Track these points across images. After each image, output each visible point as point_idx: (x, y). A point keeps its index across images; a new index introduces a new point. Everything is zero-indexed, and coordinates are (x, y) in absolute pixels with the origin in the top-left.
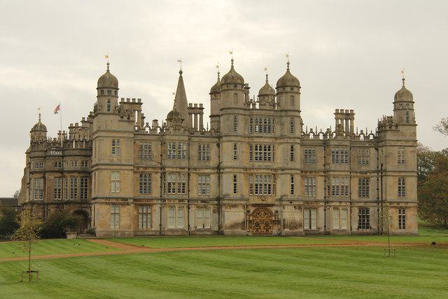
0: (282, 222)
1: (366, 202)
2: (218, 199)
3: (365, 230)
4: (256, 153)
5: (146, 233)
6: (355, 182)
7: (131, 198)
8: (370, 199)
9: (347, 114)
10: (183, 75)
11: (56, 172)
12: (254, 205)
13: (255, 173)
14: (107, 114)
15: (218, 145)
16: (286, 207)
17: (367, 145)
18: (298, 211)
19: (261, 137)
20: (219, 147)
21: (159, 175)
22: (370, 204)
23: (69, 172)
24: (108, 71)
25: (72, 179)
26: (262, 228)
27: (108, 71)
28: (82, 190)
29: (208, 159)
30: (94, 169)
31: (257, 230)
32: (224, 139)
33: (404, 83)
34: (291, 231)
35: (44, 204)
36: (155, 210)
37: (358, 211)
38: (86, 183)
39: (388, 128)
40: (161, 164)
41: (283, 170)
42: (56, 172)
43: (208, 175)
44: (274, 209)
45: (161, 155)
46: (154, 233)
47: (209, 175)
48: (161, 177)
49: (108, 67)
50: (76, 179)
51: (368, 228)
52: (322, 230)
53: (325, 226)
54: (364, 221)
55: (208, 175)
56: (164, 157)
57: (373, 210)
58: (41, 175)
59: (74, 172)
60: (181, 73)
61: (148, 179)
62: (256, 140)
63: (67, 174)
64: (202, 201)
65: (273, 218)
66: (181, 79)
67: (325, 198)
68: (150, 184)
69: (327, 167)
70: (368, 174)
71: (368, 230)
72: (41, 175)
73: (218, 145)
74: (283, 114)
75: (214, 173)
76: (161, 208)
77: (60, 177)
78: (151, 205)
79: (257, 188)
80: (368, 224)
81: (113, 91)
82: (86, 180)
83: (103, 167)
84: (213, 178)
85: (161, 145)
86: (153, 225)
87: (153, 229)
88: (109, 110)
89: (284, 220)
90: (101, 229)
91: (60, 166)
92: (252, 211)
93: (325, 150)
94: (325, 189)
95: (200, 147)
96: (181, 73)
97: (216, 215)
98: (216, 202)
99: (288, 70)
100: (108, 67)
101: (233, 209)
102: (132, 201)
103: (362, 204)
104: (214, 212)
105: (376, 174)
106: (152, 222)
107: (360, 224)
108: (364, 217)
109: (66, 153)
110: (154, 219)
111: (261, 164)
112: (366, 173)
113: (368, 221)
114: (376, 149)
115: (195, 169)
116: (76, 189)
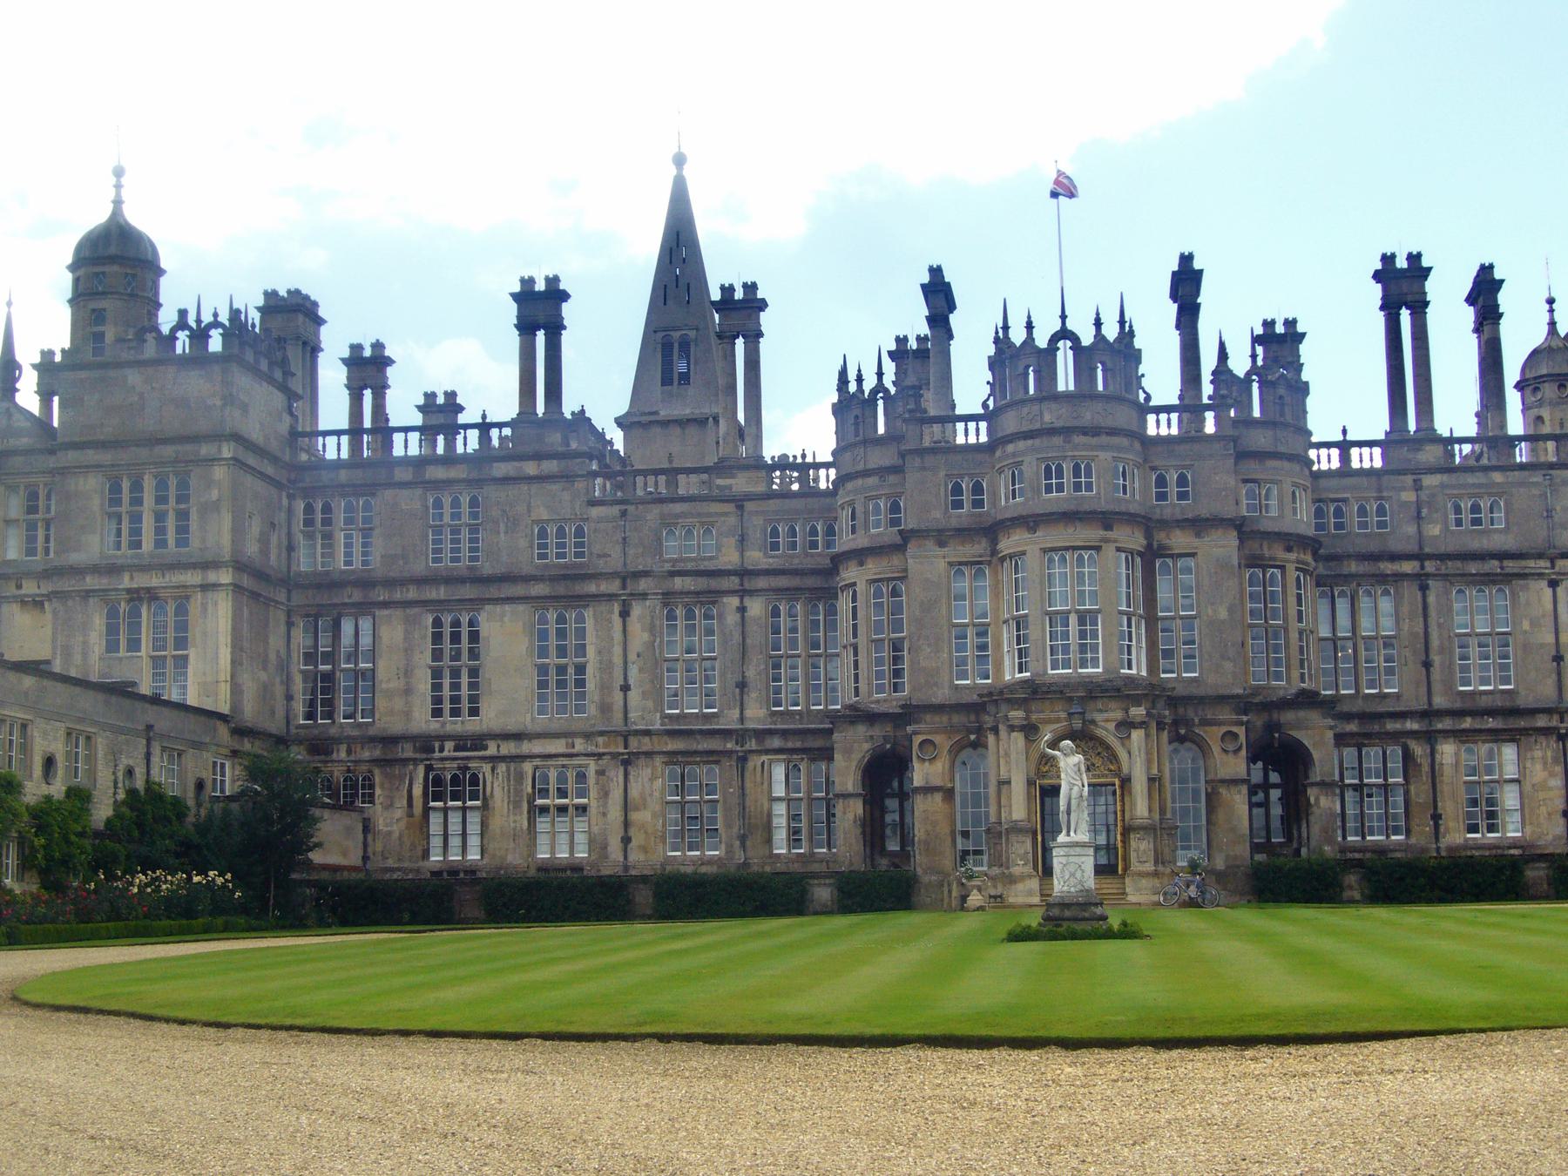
63: (1281, 554)
72: (1137, 540)
109: (1260, 440)
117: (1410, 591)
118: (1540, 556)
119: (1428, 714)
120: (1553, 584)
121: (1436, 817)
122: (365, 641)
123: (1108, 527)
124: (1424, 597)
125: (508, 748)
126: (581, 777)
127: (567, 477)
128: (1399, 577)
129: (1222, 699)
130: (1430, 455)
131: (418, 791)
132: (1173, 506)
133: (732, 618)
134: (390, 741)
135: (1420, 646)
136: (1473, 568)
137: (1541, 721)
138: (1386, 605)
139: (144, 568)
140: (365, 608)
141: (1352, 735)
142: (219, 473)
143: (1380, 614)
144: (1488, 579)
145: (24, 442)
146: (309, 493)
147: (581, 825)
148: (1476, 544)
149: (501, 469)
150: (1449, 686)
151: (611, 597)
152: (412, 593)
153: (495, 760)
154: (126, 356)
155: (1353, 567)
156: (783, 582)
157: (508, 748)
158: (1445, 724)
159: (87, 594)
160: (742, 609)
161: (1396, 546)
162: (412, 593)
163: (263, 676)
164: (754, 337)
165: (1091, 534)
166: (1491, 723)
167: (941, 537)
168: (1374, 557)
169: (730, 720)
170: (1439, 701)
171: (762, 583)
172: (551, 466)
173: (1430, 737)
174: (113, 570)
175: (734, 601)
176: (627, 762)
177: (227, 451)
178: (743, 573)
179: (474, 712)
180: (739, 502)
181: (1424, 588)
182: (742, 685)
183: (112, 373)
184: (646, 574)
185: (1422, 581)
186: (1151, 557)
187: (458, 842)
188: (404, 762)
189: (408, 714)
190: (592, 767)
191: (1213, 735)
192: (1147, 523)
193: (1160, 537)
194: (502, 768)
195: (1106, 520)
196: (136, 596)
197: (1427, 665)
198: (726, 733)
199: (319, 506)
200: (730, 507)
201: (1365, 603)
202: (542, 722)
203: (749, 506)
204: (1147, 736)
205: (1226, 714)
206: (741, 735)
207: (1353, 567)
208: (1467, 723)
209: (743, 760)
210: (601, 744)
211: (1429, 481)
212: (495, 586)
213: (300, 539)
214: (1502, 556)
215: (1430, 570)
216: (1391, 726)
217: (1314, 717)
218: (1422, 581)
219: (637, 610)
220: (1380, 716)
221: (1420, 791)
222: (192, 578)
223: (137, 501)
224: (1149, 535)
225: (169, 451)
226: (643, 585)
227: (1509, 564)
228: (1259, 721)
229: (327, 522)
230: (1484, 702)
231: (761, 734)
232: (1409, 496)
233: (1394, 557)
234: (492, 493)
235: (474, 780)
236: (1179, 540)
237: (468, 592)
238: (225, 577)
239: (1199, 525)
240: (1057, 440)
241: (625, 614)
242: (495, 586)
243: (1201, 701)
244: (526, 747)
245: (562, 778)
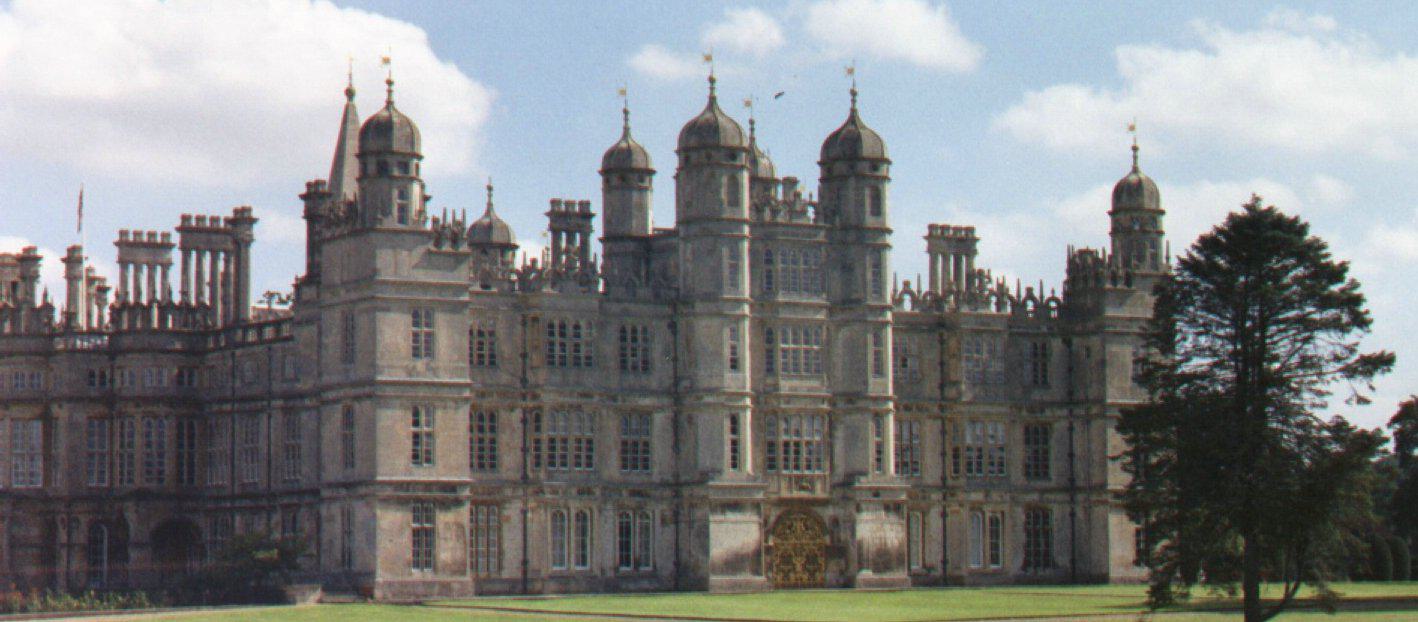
0: (853, 552)
1: (1044, 491)
2: (676, 485)
3: (1041, 573)
4: (784, 351)
5: (487, 587)
6: (1018, 433)
7: (463, 484)
8: (1053, 484)
9: (961, 240)
11: (92, 400)
12: (782, 502)
13: (784, 411)
14: (396, 232)
15: (673, 326)
16: (864, 506)
17: (1044, 329)
18: (893, 517)
19: (796, 305)
20: (674, 333)
21: (517, 415)
22: (1052, 497)
23: (141, 400)
25: (149, 424)
26: (799, 568)
28: (179, 457)
29: (646, 366)
30: (331, 395)
31: (786, 576)
32: (699, 307)
33: (1135, 158)
34: (876, 577)
35: (46, 499)
36: (508, 519)
37: (1023, 517)
38: (191, 437)
39: (1108, 286)
40: (524, 381)
41: (850, 401)
42: (92, 400)
43: (645, 416)
44: (828, 513)
45: (524, 356)
46: (506, 587)
47: (650, 413)
48: (524, 421)
49: (390, 92)
50: (161, 425)
51: (1046, 565)
52: (938, 573)
53: (944, 562)
54: (1037, 544)
55: (645, 416)
56: (536, 359)
57: (1058, 512)
60: (350, 93)
61: (486, 424)
62: (784, 314)
63: (130, 409)
64: (634, 493)
65: (827, 540)
67: (944, 479)
68: (493, 441)
69: (951, 392)
70: (1048, 413)
71: (1048, 572)
72: (37, 410)
73: (673, 326)
74: (852, 236)
75: (661, 408)
76: (524, 512)
77: (102, 418)
78: (500, 504)
79: (553, 448)
80: (1047, 554)
82: (191, 427)
83: (390, 391)
84: (660, 419)
85: (524, 324)
86: (506, 564)
87: (505, 574)
88: (402, 220)
89: (860, 546)
90: (389, 577)
91: (103, 383)
92: (772, 519)
93: (942, 342)
94: (943, 454)
95: (623, 330)
96: (350, 93)
97: (670, 529)
98: (668, 493)
99: (853, 111)
100: (390, 92)
101: (731, 516)
102: (466, 492)
103: (1034, 497)
104: (663, 521)
105: (1065, 412)
106: (501, 553)
107: (1027, 553)
108: (1037, 533)
109: (126, 341)
110: (506, 545)
111: (796, 383)
112: (1042, 411)
113: (1047, 544)
114: (1064, 341)
115: (614, 399)
116: (161, 455)
118: (263, 399)
119: (233, 497)
120: (270, 417)
155: (215, 408)
158: (237, 504)
161: (229, 393)
170: (237, 490)
173: (232, 510)
181: (233, 421)
186: (47, 419)
207: (215, 408)
211: (238, 352)
214: (253, 399)
232: (230, 363)
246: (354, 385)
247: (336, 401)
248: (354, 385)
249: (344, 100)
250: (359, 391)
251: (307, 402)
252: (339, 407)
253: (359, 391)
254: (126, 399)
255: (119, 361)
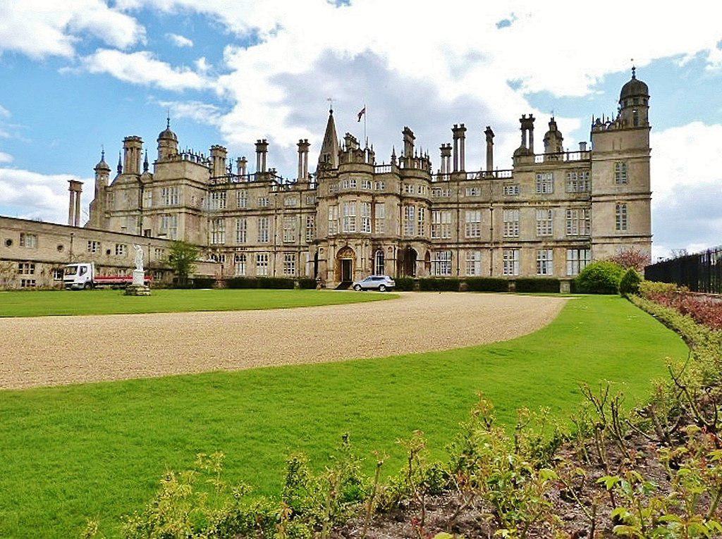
10: (333, 114)
23: (416, 200)
24: (634, 77)
27: (634, 77)
30: (602, 199)
49: (634, 73)
58: (370, 199)
59: (422, 200)
60: (331, 111)
63: (413, 202)
66: (331, 117)
72: (370, 199)
81: (641, 102)
96: (331, 111)
100: (634, 73)
109: (409, 173)
117: (455, 211)
118: (488, 203)
120: (492, 210)
121: (458, 270)
122: (223, 224)
123: (358, 196)
124: (458, 214)
125: (251, 249)
126: (266, 257)
127: (264, 187)
128: (452, 208)
129: (388, 239)
130: (462, 176)
131: (233, 259)
132: (381, 190)
133: (299, 219)
134: (227, 248)
135: (456, 226)
136: (471, 206)
137: (486, 245)
138: (449, 214)
139: (168, 209)
140: (224, 217)
141: (438, 249)
142: (183, 187)
143: (447, 218)
144: (476, 209)
145: (148, 181)
146: (213, 191)
147: (265, 267)
148: (473, 200)
149: (251, 185)
150: (463, 237)
151: (273, 214)
152: (233, 214)
153: (248, 252)
154: (167, 161)
155: (441, 206)
156: (309, 211)
157: (251, 249)
159: (158, 214)
160: (301, 217)
161: (452, 200)
162: (233, 214)
163: (198, 233)
164: (307, 151)
165: (354, 198)
166: (475, 246)
167: (327, 199)
168: (447, 203)
169: (297, 244)
170: (460, 240)
171: (305, 211)
172: (262, 184)
174: (163, 209)
175: (299, 215)
176: (275, 253)
177: (185, 182)
178: (301, 209)
179: (245, 241)
180: (301, 191)
181: (458, 211)
182: (300, 235)
183: (164, 165)
184: (280, 209)
185: (458, 209)
187: (242, 271)
188: (230, 252)
189: (232, 242)
190: (268, 254)
191: (385, 248)
192: (373, 196)
193: (376, 198)
194: (250, 254)
195: (358, 194)
196: (167, 215)
197: (458, 231)
198: (296, 247)
199: (215, 194)
200: (299, 193)
201: (443, 215)
202: (259, 244)
203: (303, 193)
204: (362, 248)
205: (389, 243)
206: (299, 247)
208: (468, 246)
209: (300, 253)
210: (270, 249)
211: (461, 183)
212: (248, 212)
213: (211, 202)
214: (478, 203)
215: (457, 206)
216: (448, 246)
217: (419, 244)
218: (458, 209)
219: (278, 217)
220: (445, 244)
221: (454, 263)
222: (178, 210)
223: (168, 194)
224: (373, 198)
225: (173, 182)
226: (280, 212)
227: (481, 205)
228: (405, 244)
229: (217, 198)
230: (472, 241)
231: (303, 247)
233: (451, 203)
234: (249, 190)
235: (245, 257)
236: (380, 199)
237: (244, 213)
238: (184, 210)
239: (386, 195)
240: (347, 174)
241: (276, 218)
242: (248, 212)
243: (383, 240)
244: (255, 249)
245: (262, 257)
246: (628, 194)
247: (614, 200)
248: (628, 194)
249: (330, 114)
250: (634, 197)
251: (525, 204)
252: (613, 204)
253: (630, 197)
254: (412, 198)
255: (406, 181)
